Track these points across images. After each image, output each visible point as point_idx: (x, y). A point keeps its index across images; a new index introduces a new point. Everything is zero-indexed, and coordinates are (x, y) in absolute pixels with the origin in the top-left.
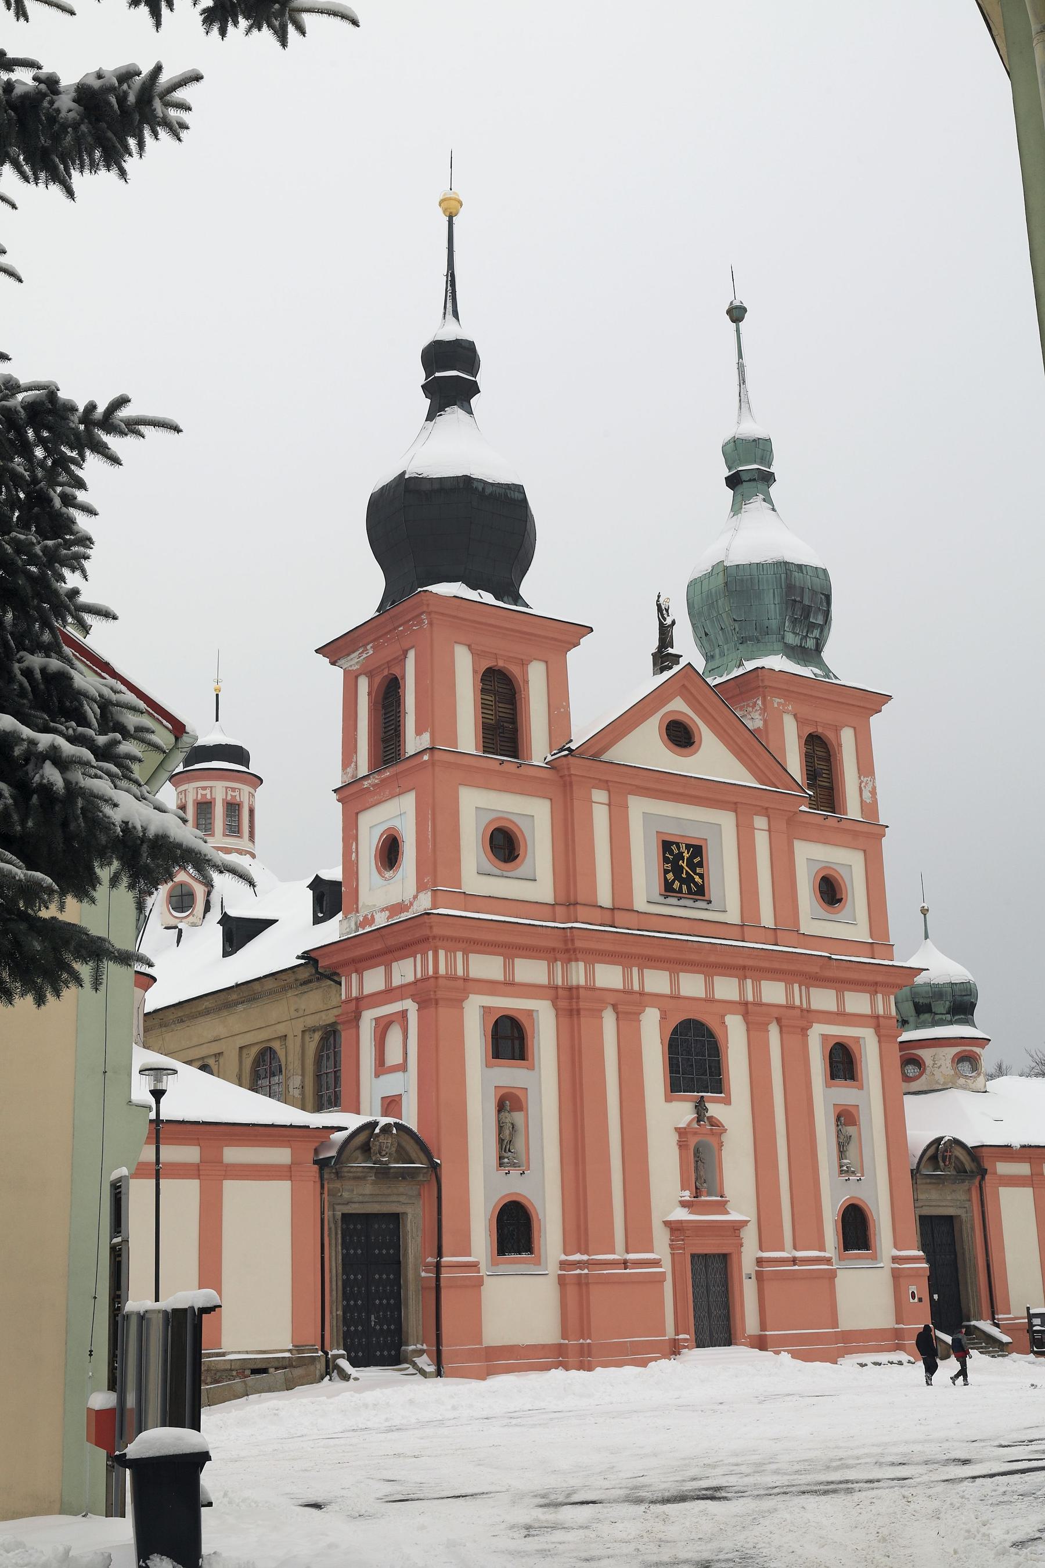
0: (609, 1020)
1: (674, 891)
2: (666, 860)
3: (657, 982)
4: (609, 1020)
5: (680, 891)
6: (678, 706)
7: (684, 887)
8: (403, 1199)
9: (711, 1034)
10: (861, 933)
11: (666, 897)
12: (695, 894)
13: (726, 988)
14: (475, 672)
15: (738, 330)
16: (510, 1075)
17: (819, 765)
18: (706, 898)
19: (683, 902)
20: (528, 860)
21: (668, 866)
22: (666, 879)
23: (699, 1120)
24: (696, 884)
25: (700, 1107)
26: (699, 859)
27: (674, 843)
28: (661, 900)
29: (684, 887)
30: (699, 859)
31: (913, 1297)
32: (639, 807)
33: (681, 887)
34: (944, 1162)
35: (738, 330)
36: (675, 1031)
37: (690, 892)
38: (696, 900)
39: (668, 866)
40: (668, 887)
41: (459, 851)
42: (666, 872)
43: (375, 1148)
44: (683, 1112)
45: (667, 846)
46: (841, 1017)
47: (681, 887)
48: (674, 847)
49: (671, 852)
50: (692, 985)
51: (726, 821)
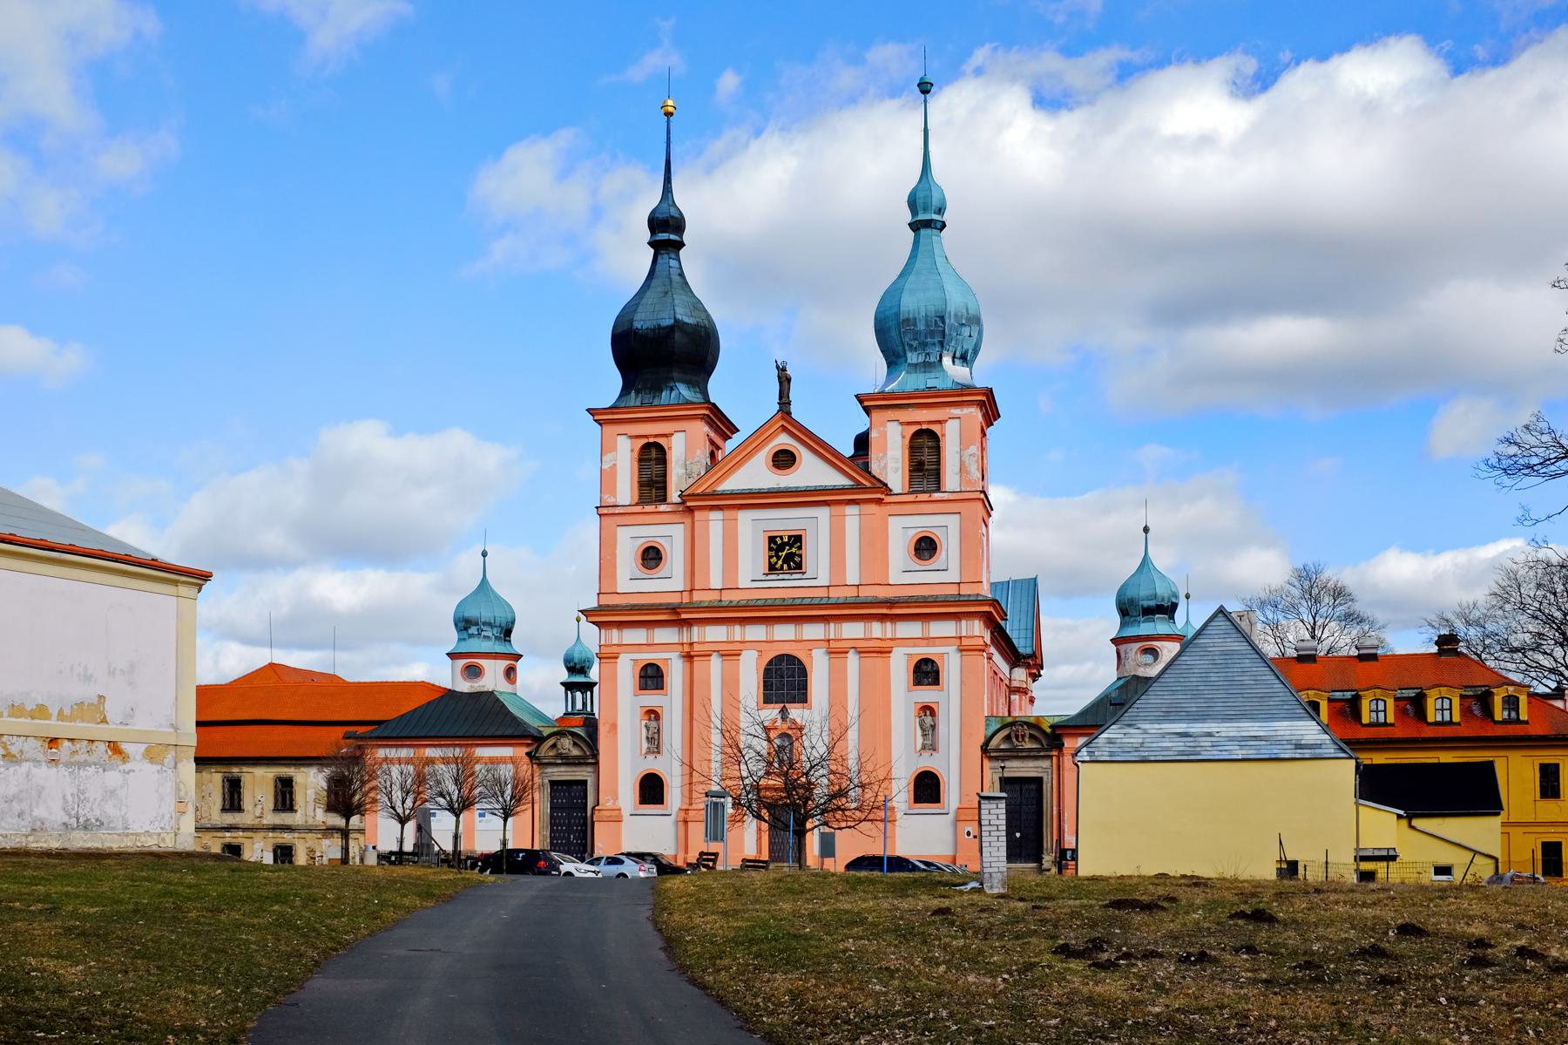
0: (715, 662)
1: (777, 569)
2: (771, 549)
3: (756, 632)
4: (715, 662)
5: (782, 568)
6: (784, 441)
7: (785, 566)
8: (584, 773)
9: (800, 663)
10: (953, 575)
11: (767, 574)
12: (795, 569)
13: (814, 631)
14: (632, 451)
15: (925, 101)
16: (652, 699)
17: (926, 457)
18: (803, 570)
19: (781, 577)
20: (668, 565)
21: (773, 553)
22: (770, 562)
23: (784, 719)
24: (795, 562)
25: (784, 713)
26: (799, 544)
27: (777, 537)
28: (764, 577)
29: (785, 566)
30: (799, 544)
31: (969, 834)
32: (745, 518)
33: (782, 566)
34: (1017, 740)
35: (925, 101)
36: (770, 663)
37: (789, 568)
38: (791, 574)
39: (773, 553)
40: (772, 567)
41: (615, 567)
42: (770, 557)
43: (559, 747)
44: (771, 713)
45: (772, 539)
46: (928, 640)
47: (782, 566)
48: (778, 540)
49: (775, 543)
50: (784, 632)
51: (823, 513)
